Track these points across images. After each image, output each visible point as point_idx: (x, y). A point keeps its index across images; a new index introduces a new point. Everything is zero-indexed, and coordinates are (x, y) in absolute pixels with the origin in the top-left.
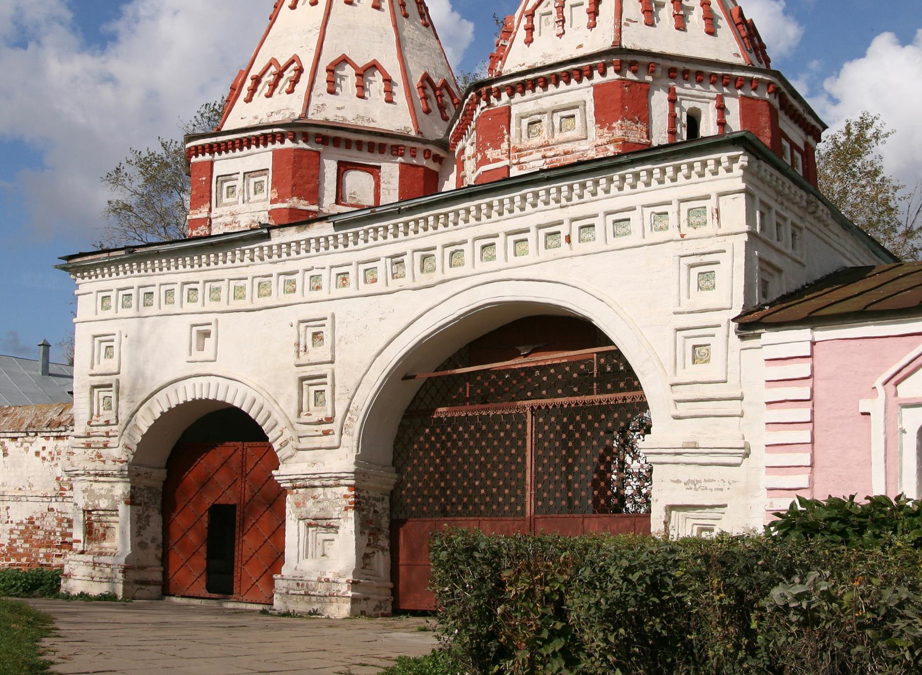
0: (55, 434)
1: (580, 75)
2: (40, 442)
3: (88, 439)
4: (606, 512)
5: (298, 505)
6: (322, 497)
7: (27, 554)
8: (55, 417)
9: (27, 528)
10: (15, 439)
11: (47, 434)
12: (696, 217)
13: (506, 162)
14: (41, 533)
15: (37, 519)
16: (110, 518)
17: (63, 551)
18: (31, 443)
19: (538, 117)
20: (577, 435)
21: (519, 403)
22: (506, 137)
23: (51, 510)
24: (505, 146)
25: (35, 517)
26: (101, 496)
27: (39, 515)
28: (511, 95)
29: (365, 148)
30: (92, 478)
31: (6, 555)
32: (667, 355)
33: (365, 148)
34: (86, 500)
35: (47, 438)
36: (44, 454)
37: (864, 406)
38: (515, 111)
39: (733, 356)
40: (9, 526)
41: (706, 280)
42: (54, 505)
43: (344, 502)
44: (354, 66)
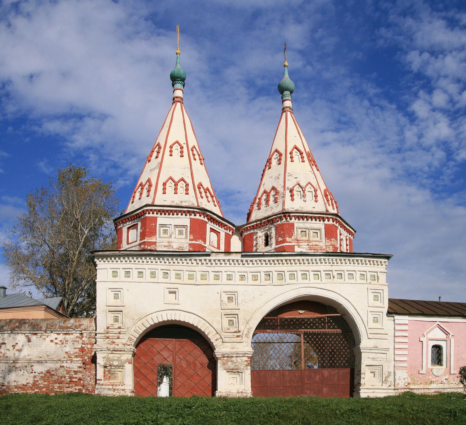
0: (64, 332)
2: (53, 336)
3: (119, 335)
4: (334, 367)
5: (224, 364)
6: (235, 361)
7: (47, 387)
9: (45, 375)
10: (36, 334)
11: (59, 332)
13: (295, 244)
15: (53, 371)
16: (116, 370)
17: (70, 385)
18: (47, 336)
19: (305, 230)
20: (320, 342)
21: (299, 330)
22: (294, 234)
24: (293, 237)
25: (51, 370)
26: (114, 360)
27: (54, 369)
30: (110, 352)
31: (31, 388)
34: (105, 362)
35: (59, 334)
38: (296, 225)
40: (33, 374)
42: (65, 365)
43: (246, 363)
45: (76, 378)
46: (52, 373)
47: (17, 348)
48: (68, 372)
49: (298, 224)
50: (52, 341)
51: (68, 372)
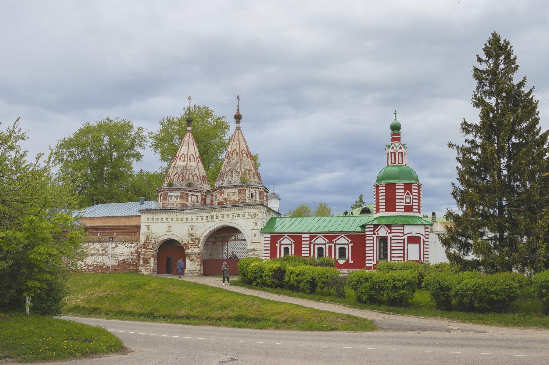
2: (127, 244)
12: (255, 215)
38: (225, 191)
39: (260, 236)
41: (256, 225)
42: (131, 257)
44: (192, 175)
45: (135, 263)
46: (126, 260)
48: (132, 260)
49: (226, 191)
50: (126, 246)
51: (132, 260)
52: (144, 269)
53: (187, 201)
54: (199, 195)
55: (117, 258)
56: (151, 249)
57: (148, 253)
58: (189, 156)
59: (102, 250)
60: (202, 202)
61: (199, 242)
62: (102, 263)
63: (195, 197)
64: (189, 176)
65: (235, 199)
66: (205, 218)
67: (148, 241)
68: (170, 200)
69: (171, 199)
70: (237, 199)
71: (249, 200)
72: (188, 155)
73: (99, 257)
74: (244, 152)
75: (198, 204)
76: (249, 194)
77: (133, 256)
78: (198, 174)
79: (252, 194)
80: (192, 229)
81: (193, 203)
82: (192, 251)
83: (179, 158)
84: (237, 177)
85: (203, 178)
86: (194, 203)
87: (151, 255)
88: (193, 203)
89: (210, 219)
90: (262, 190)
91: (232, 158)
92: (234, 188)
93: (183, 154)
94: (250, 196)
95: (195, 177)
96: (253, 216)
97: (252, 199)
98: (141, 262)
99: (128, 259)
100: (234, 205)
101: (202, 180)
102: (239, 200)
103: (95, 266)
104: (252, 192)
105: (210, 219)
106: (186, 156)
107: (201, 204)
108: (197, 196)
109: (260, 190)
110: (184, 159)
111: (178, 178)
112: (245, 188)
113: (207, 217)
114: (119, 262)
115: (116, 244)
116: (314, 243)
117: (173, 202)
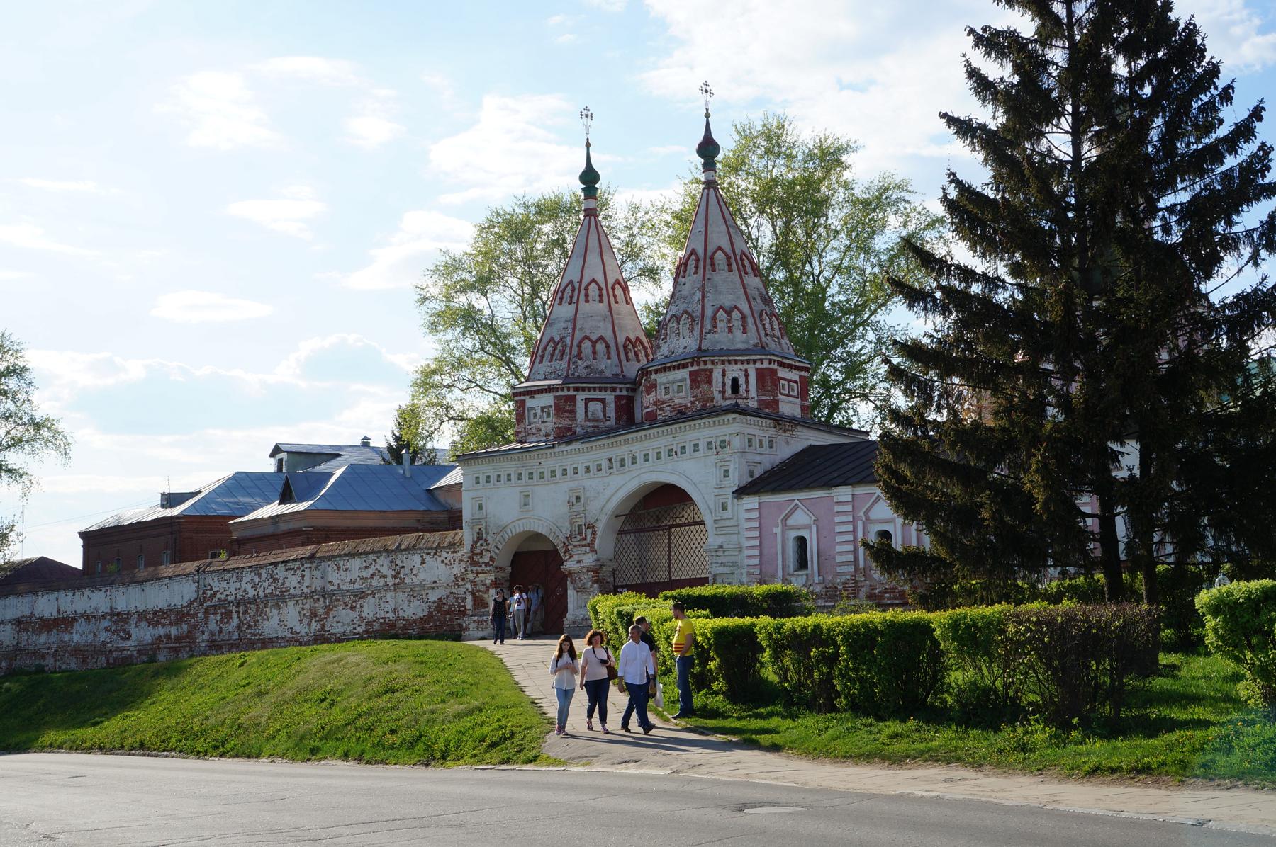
1: (685, 366)
2: (444, 555)
8: (452, 540)
10: (429, 554)
12: (724, 445)
14: (447, 607)
19: (667, 385)
23: (452, 593)
28: (656, 373)
29: (597, 390)
32: (712, 507)
33: (597, 390)
35: (448, 553)
36: (446, 561)
37: (775, 530)
39: (736, 508)
42: (454, 590)
44: (591, 340)
46: (444, 601)
47: (414, 572)
48: (457, 599)
49: (662, 378)
50: (442, 562)
51: (457, 599)
52: (474, 621)
53: (574, 419)
54: (610, 397)
55: (424, 597)
56: (487, 564)
57: (482, 577)
58: (583, 287)
59: (394, 576)
60: (618, 419)
61: (594, 534)
62: (394, 611)
63: (599, 406)
64: (579, 346)
65: (684, 402)
66: (604, 464)
67: (481, 542)
68: (532, 420)
69: (535, 415)
70: (687, 401)
71: (724, 399)
72: (580, 282)
73: (390, 595)
74: (719, 255)
75: (608, 423)
76: (724, 384)
77: (459, 587)
78: (608, 335)
79: (735, 382)
80: (578, 498)
81: (591, 424)
82: (579, 562)
83: (560, 294)
84: (687, 333)
85: (625, 347)
86: (596, 424)
87: (488, 582)
88: (591, 424)
89: (616, 465)
90: (766, 365)
91: (684, 277)
92: (678, 367)
93: (571, 282)
94: (729, 389)
95: (600, 347)
96: (718, 447)
97: (733, 396)
98: (469, 604)
99: (448, 596)
100: (681, 416)
101: (622, 353)
102: (692, 403)
103: (381, 623)
104: (735, 375)
105: (616, 465)
106: (577, 286)
107: (616, 423)
108: (603, 401)
109: (758, 365)
110: (572, 297)
111: (552, 355)
112: (709, 366)
113: (610, 460)
114: (430, 607)
115: (422, 557)
116: (867, 518)
117: (538, 425)
